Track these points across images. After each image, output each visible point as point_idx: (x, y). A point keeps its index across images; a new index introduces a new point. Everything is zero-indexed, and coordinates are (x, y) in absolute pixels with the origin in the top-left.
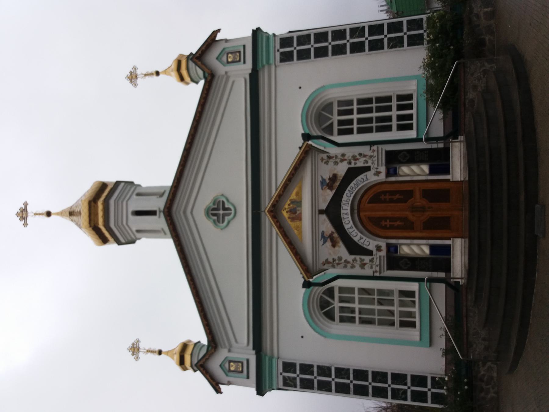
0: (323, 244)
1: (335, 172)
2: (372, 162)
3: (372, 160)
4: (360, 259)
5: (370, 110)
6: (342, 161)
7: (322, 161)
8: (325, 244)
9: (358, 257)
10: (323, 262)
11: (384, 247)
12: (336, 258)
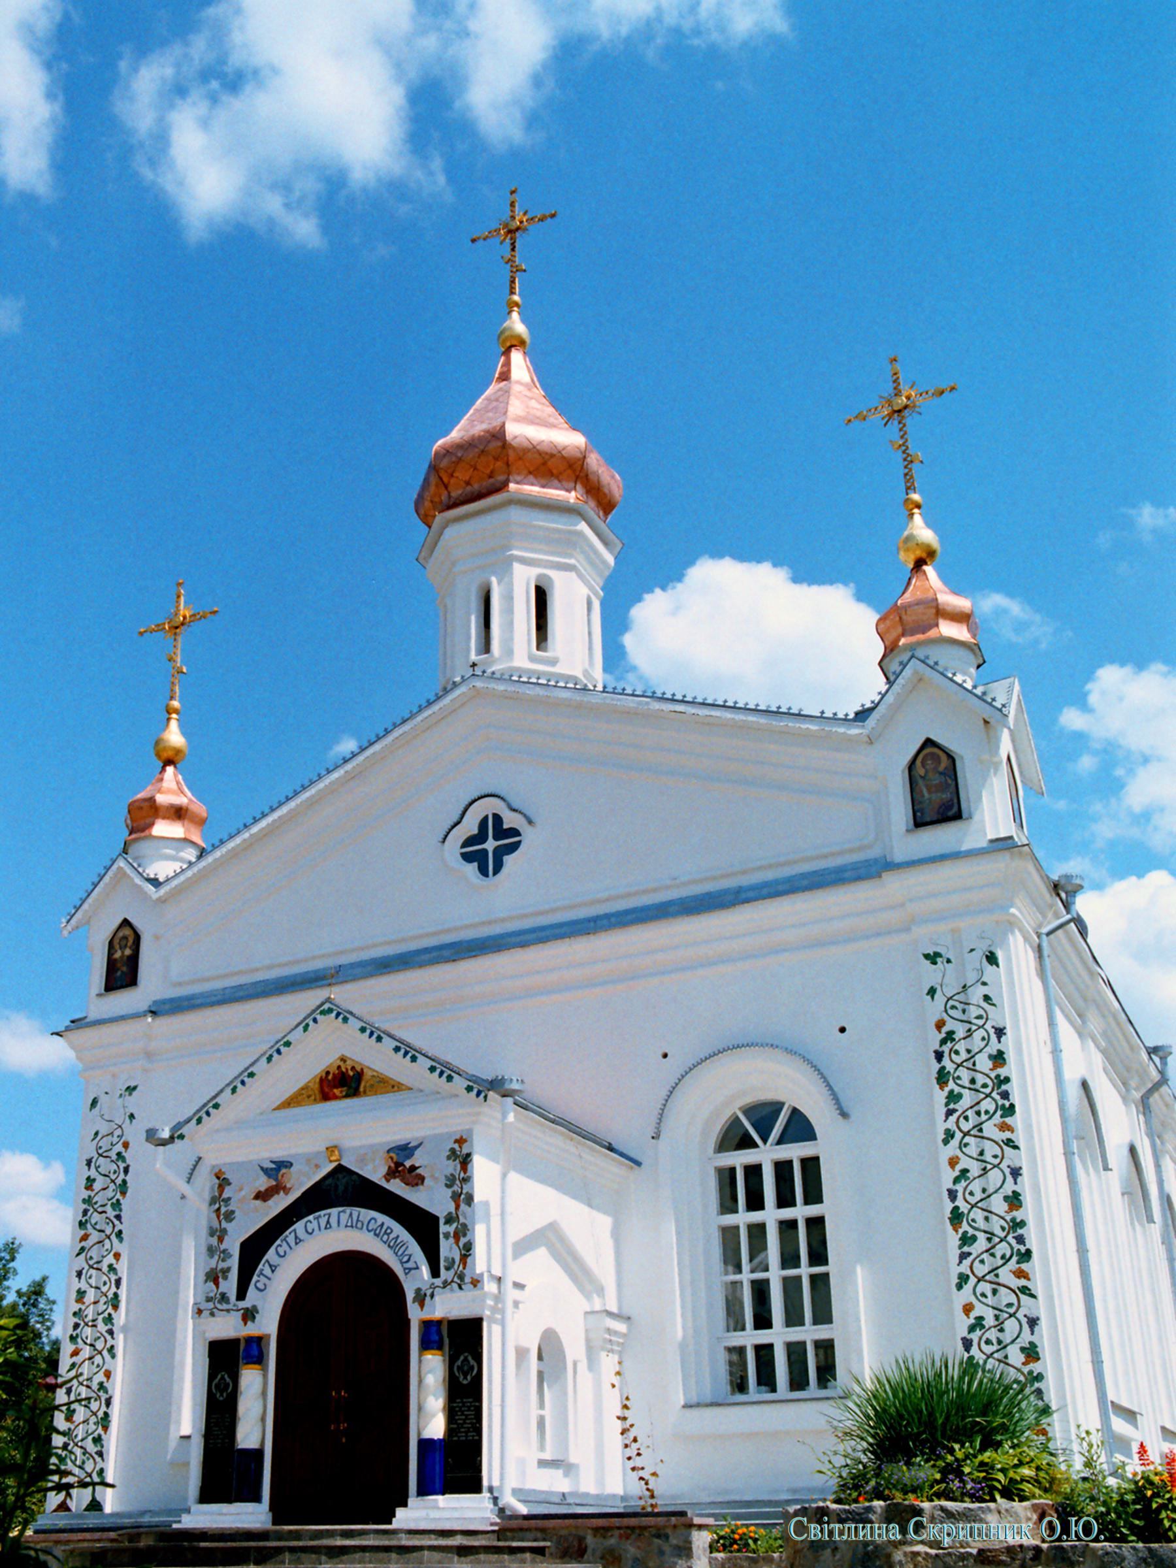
0: (262, 1168)
2: (449, 1280)
3: (452, 1281)
4: (229, 1269)
5: (789, 1259)
6: (456, 1197)
7: (456, 1141)
8: (262, 1173)
10: (224, 1173)
11: (252, 1330)
12: (230, 1208)
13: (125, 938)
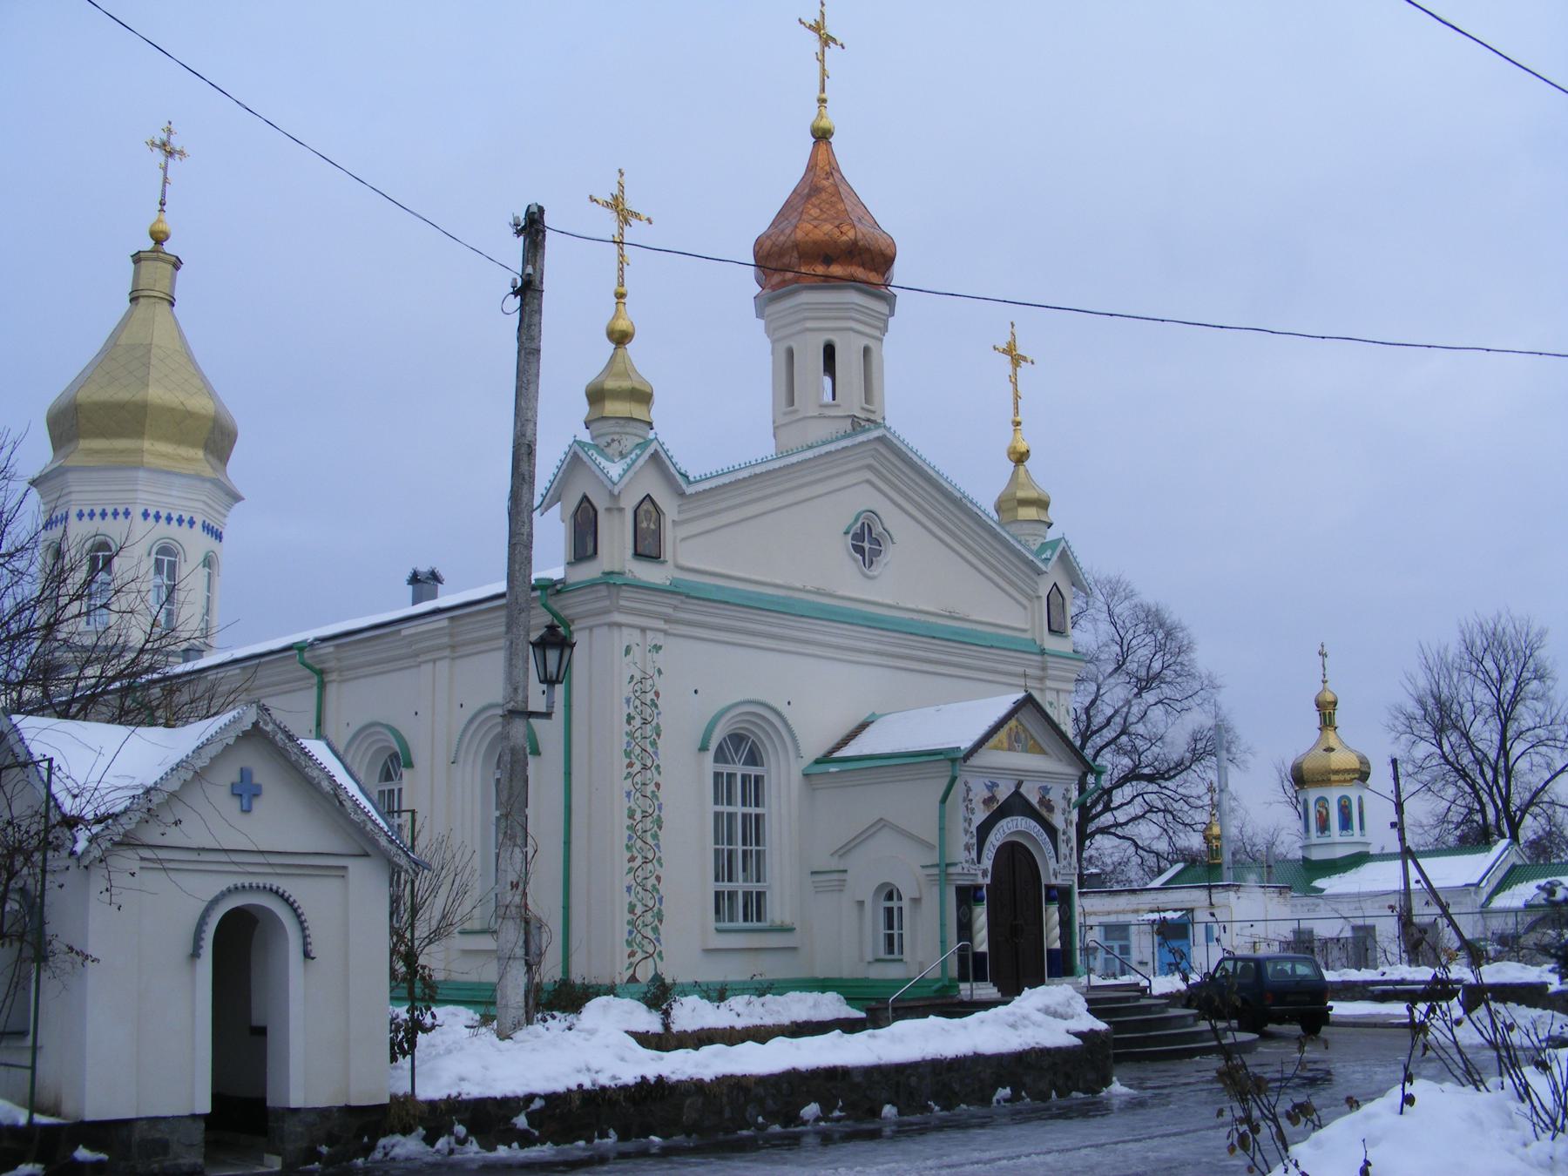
1: (1056, 810)
6: (1066, 820)
9: (974, 840)
13: (647, 512)
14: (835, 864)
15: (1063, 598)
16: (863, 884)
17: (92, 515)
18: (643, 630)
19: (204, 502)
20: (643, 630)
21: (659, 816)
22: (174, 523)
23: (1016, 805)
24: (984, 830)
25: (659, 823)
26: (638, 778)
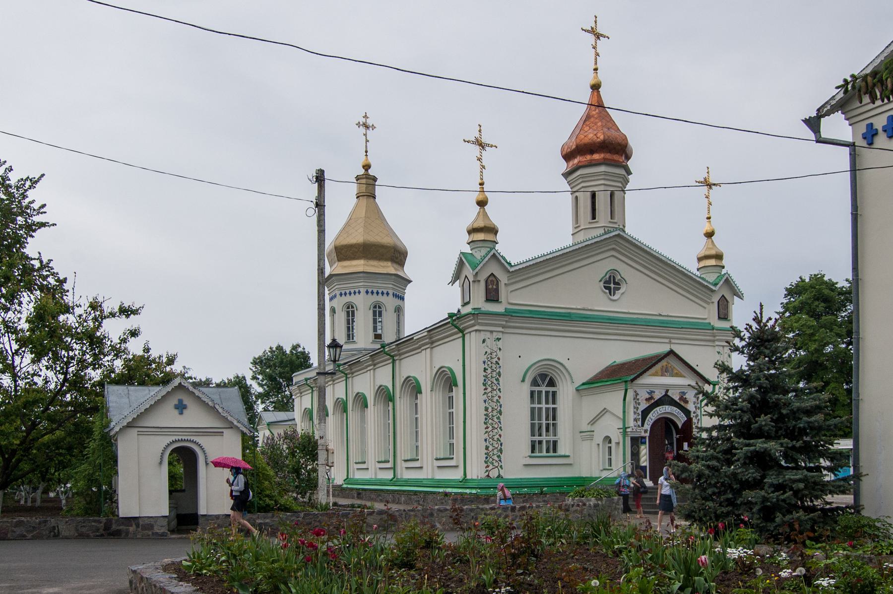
6: (696, 407)
9: (640, 417)
12: (640, 401)
14: (589, 428)
15: (718, 302)
16: (599, 438)
17: (345, 294)
18: (492, 332)
19: (393, 284)
20: (492, 332)
21: (500, 410)
22: (380, 295)
23: (666, 400)
24: (645, 413)
25: (500, 413)
26: (490, 394)
